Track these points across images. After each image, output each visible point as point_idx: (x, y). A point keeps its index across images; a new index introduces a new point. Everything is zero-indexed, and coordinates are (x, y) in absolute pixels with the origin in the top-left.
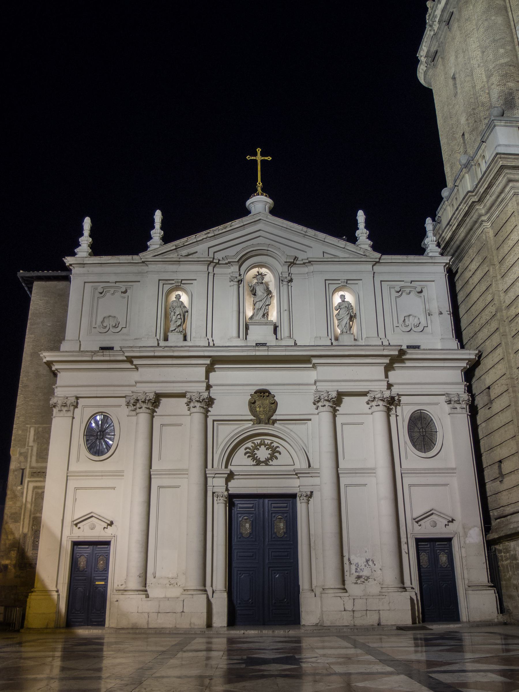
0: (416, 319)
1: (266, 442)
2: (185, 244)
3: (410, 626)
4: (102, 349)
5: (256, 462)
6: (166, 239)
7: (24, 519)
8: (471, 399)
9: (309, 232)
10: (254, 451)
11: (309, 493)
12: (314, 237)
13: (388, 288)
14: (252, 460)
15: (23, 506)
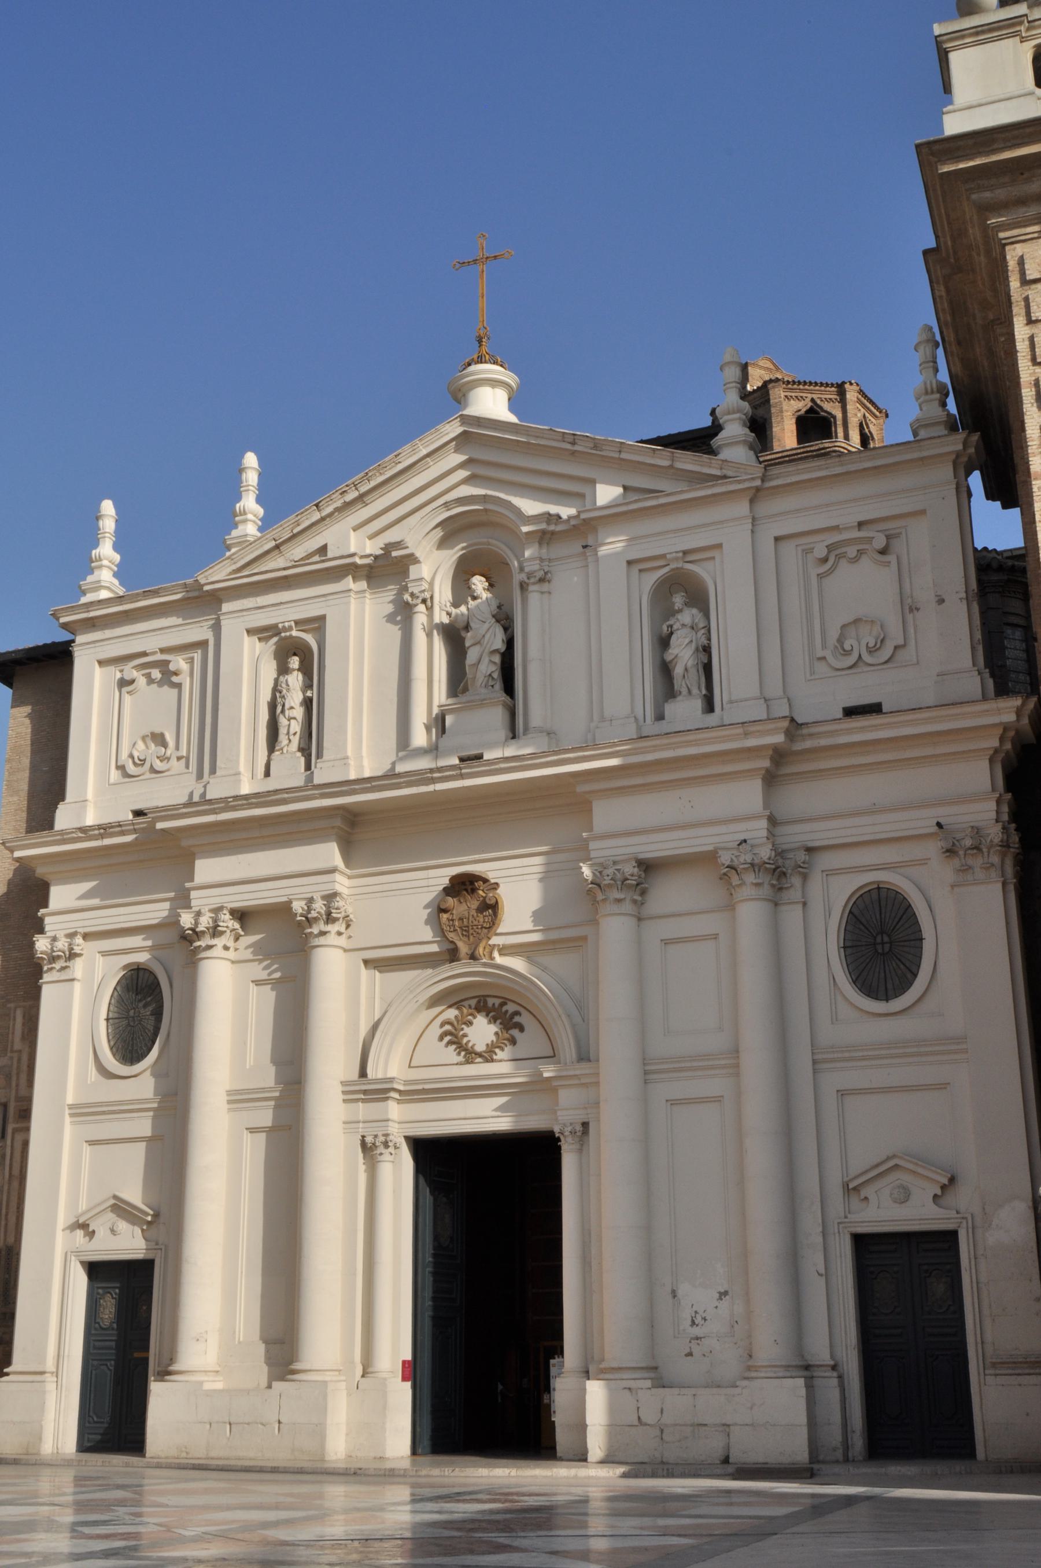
0: (876, 629)
1: (491, 1002)
2: (295, 531)
3: (805, 1466)
4: (138, 813)
5: (465, 1056)
6: (265, 525)
7: (7, 1214)
8: (1015, 838)
9: (579, 442)
10: (462, 1029)
11: (579, 1128)
12: (594, 452)
13: (800, 552)
14: (455, 1050)
15: (6, 1188)
